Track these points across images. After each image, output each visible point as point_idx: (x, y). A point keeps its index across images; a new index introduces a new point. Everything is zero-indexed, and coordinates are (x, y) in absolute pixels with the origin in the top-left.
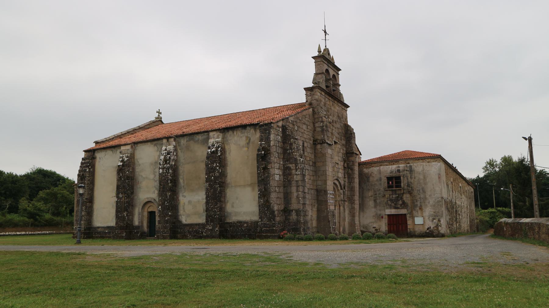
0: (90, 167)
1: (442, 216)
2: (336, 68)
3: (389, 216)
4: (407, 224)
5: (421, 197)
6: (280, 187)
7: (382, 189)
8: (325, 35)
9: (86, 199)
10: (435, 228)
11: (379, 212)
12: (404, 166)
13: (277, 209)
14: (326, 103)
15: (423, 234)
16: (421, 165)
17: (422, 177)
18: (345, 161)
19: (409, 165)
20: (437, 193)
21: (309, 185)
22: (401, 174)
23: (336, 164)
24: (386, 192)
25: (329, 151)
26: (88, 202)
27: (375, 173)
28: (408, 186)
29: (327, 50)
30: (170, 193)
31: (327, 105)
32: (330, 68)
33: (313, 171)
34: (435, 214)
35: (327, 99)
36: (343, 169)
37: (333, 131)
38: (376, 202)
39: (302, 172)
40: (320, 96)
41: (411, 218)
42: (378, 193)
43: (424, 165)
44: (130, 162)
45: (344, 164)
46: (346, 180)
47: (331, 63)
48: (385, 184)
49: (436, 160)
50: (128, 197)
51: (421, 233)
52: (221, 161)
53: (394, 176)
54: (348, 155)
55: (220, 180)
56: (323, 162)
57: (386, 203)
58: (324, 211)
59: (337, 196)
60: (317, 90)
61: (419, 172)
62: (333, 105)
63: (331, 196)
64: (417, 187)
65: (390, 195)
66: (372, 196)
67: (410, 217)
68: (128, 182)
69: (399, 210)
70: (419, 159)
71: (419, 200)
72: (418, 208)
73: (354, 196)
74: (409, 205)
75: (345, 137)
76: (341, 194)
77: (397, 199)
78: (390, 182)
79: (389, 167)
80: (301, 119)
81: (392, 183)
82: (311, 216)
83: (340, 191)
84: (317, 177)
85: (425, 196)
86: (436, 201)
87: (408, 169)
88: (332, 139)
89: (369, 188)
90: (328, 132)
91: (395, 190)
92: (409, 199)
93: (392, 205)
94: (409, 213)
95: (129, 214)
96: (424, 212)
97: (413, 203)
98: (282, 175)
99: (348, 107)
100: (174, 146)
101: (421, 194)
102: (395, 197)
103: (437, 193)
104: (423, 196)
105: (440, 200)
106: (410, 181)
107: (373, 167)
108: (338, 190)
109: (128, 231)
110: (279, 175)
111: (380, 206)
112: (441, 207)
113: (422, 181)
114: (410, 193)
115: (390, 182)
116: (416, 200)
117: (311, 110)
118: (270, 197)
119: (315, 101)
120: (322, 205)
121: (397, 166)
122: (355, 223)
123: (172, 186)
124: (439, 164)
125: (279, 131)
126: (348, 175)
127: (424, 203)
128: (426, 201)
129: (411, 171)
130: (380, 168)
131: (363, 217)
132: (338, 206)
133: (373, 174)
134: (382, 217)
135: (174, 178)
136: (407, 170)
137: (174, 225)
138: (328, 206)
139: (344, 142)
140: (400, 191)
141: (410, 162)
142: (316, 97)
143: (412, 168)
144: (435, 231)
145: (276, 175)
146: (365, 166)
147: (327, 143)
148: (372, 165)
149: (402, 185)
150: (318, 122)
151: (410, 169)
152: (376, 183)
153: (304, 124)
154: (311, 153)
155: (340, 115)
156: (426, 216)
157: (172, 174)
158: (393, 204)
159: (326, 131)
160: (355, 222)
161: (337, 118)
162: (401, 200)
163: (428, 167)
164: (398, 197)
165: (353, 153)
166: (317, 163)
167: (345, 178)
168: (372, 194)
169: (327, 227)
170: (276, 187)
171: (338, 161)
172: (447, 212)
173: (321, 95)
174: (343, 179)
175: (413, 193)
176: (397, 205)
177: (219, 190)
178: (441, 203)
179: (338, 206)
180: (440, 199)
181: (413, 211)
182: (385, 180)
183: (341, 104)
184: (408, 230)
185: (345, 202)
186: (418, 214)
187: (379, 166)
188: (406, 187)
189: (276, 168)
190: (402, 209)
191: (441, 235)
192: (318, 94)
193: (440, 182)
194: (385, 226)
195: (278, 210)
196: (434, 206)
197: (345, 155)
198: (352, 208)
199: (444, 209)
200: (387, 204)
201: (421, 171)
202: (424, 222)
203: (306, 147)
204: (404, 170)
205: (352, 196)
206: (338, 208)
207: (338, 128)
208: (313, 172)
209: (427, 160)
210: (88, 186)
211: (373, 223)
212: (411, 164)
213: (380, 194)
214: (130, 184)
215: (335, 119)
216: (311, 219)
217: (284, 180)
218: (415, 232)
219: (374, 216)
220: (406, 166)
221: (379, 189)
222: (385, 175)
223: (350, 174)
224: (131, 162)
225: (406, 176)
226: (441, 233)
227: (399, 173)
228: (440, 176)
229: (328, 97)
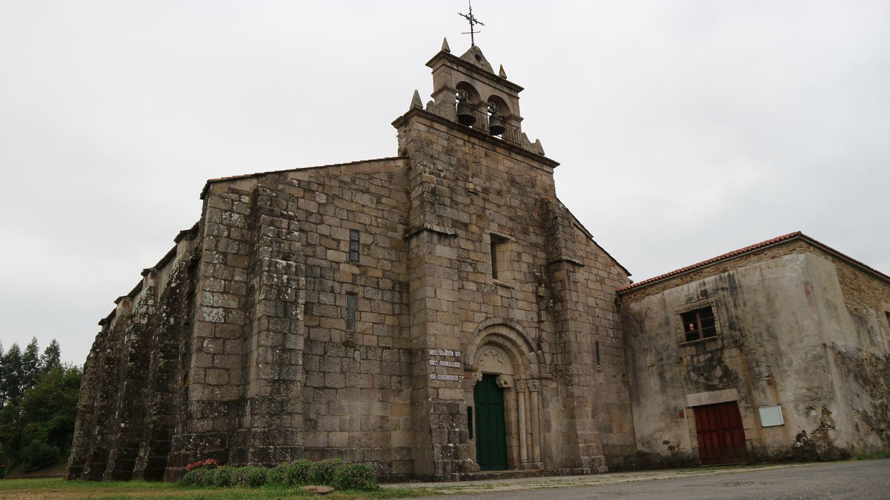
0: (98, 350)
1: (832, 399)
2: (502, 83)
3: (697, 409)
4: (742, 427)
5: (768, 350)
6: (225, 340)
7: (673, 345)
8: (472, 25)
9: (84, 406)
10: (818, 435)
11: (673, 403)
12: (716, 280)
13: (205, 398)
14: (456, 148)
15: (786, 452)
16: (756, 268)
17: (761, 299)
18: (539, 282)
19: (726, 274)
20: (808, 336)
21: (376, 337)
22: (712, 299)
23: (499, 287)
24: (683, 349)
25: (444, 251)
26: (88, 413)
27: (655, 308)
28: (732, 327)
29: (476, 53)
30: (127, 381)
31: (460, 154)
32: (477, 81)
33: (393, 303)
34: (811, 394)
35: (460, 142)
36: (535, 301)
37: (487, 212)
38: (665, 377)
39: (278, 295)
40: (428, 132)
41: (751, 410)
42: (665, 355)
43: (763, 267)
44: (117, 332)
45: (537, 288)
46: (547, 327)
47: (482, 73)
48: (679, 331)
49: (791, 248)
50: (107, 397)
51: (782, 450)
52: (175, 300)
53: (695, 308)
54: (552, 267)
55: (167, 342)
56: (420, 279)
57: (685, 379)
58: (422, 403)
59: (522, 368)
60: (415, 119)
61: (753, 288)
62: (486, 155)
64: (754, 327)
65: (692, 357)
66: (654, 365)
67: (748, 407)
68: (108, 368)
69: (717, 392)
70: (748, 255)
71: (763, 359)
72: (764, 383)
73: (570, 364)
74: (741, 377)
75: (542, 227)
76: (531, 363)
77: (710, 366)
78: (691, 325)
79: (683, 290)
80: (347, 179)
81: (696, 327)
82: (382, 418)
83: (527, 355)
84: (412, 317)
85: (778, 347)
86: (808, 356)
87: (725, 287)
88: (482, 229)
89: (646, 347)
90: (442, 207)
91: (703, 344)
92: (739, 360)
93: (700, 380)
94: (742, 399)
95: (105, 431)
96: (781, 390)
97: (750, 369)
98: (238, 308)
99: (554, 164)
100: (150, 287)
101: (765, 343)
102: (705, 361)
103: (808, 336)
104: (772, 347)
105: (821, 354)
106: (734, 313)
107: (648, 295)
108: (522, 353)
109: (99, 463)
110: (221, 310)
111: (672, 387)
112: (824, 371)
113: (763, 310)
114: (739, 345)
115: (691, 325)
116: (757, 361)
117: (400, 163)
118: (190, 367)
119: (412, 143)
120: (419, 389)
121: (700, 284)
122: (577, 435)
123: (134, 367)
124: (802, 257)
125: (240, 201)
126: (555, 316)
127: (778, 366)
128: (782, 361)
129: (733, 287)
130: (663, 294)
131: (640, 417)
132: (524, 392)
133: (651, 311)
134: (681, 415)
135: (144, 352)
136: (723, 289)
137: (132, 449)
138: (430, 391)
139: (540, 240)
140: (713, 343)
141: (728, 265)
142: (414, 134)
143: (734, 282)
144: (819, 443)
145: (206, 308)
146: (632, 296)
147: (431, 231)
148: (647, 292)
149: (717, 326)
150: (415, 187)
151: (730, 283)
152: (659, 332)
153: (364, 192)
154: (392, 262)
155: (518, 179)
156: (787, 402)
157: (136, 343)
158: (702, 380)
159: (433, 204)
160: (576, 430)
161: (508, 184)
162: (718, 367)
163: (774, 270)
164: (711, 359)
165: (560, 261)
166: (411, 283)
167: (540, 322)
168: (654, 359)
169: (428, 446)
170: (204, 339)
171: (514, 281)
172: (855, 386)
173: (432, 130)
174: (536, 325)
175: (746, 344)
176: (712, 380)
177: (161, 364)
178: (823, 361)
179: (524, 392)
180: (818, 349)
181: (753, 392)
182: (678, 322)
183: (525, 156)
184: (748, 443)
185: (544, 382)
186: (766, 397)
187: (661, 290)
188: (726, 332)
189: (208, 289)
190: (725, 389)
191: (839, 454)
192: (419, 126)
193: (811, 303)
194: (691, 437)
195: (208, 404)
196: (805, 373)
197: (542, 268)
198: (567, 396)
199: (835, 376)
200: (687, 379)
201: (759, 284)
202: (785, 418)
203: (370, 245)
204: (718, 289)
205: (566, 365)
206: (527, 397)
207: (510, 207)
208: (397, 306)
209: (770, 254)
210: (90, 384)
211: (663, 430)
212: (731, 272)
213: (669, 357)
214: (116, 372)
215: (496, 185)
216: (381, 427)
217: (244, 321)
218: (765, 448)
219: (662, 413)
220: (721, 278)
221: (667, 344)
222: (676, 309)
223: (558, 312)
224: (120, 331)
225: (723, 303)
226: (837, 448)
227: (707, 298)
228: (809, 288)
229: (466, 138)
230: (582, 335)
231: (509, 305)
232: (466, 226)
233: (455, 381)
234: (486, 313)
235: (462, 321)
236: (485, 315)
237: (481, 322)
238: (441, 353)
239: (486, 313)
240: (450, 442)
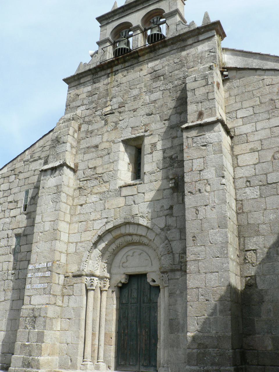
63: (40, 274)
183: (172, 44)
229: (109, 71)
230: (208, 208)
231: (134, 202)
232: (97, 147)
233: (44, 289)
234: (107, 218)
235: (81, 232)
236: (106, 220)
237: (100, 228)
238: (37, 266)
239: (107, 218)
240: (28, 341)
